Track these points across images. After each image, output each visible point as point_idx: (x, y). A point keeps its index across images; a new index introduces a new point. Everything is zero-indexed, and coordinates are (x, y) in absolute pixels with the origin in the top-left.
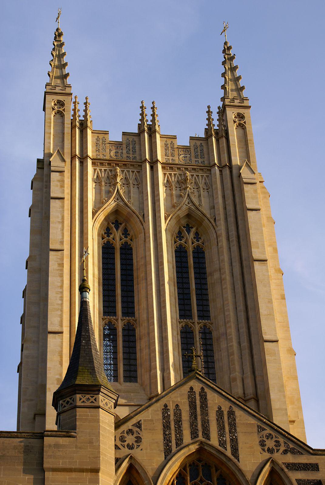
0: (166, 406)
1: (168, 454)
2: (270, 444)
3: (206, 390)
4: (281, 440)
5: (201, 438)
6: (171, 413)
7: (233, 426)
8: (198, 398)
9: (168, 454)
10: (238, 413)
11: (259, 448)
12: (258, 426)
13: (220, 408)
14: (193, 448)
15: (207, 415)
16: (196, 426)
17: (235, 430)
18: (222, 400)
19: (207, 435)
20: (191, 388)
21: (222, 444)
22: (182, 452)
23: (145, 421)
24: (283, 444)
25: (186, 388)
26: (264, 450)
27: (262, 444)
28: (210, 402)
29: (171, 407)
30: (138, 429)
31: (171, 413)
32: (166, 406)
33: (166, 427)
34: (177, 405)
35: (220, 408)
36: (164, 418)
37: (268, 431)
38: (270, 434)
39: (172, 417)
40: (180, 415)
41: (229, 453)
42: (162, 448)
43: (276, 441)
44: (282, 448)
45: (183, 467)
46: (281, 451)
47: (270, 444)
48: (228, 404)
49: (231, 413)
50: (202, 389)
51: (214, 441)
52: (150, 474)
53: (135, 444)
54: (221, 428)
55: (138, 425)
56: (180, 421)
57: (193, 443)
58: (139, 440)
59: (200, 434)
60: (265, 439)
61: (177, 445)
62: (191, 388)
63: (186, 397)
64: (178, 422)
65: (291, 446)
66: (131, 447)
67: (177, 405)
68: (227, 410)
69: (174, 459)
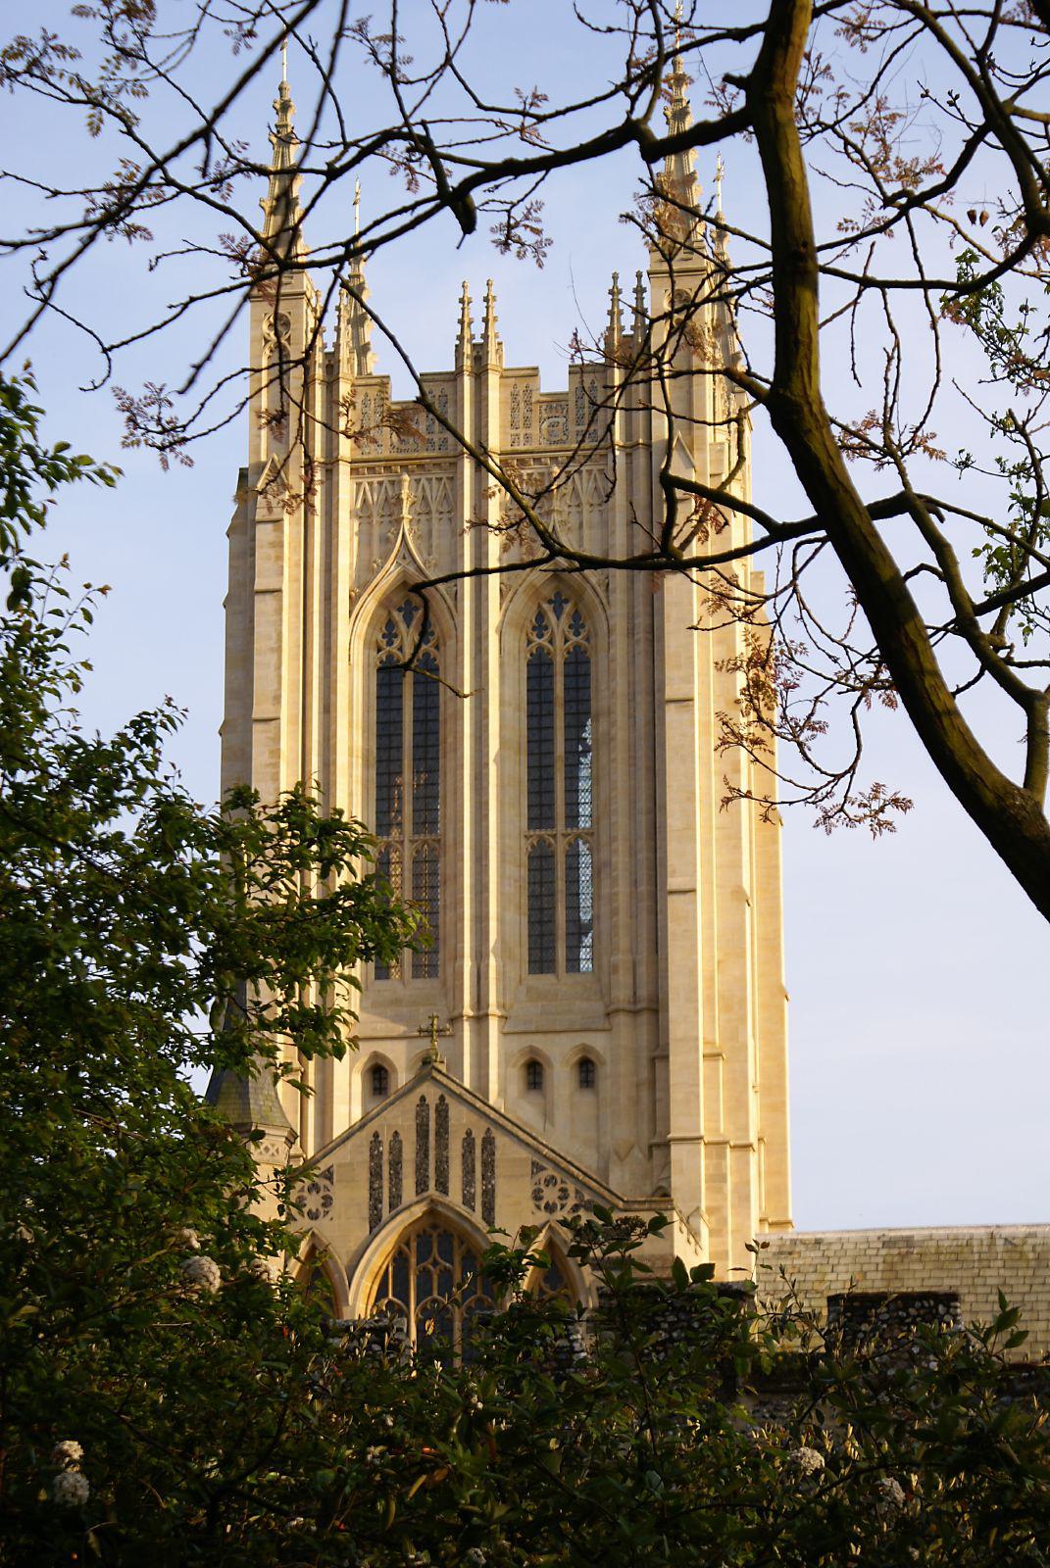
0: (376, 1135)
1: (376, 1223)
2: (551, 1195)
3: (448, 1100)
4: (571, 1187)
5: (432, 1190)
6: (385, 1148)
7: (489, 1166)
8: (433, 1115)
9: (376, 1223)
10: (501, 1140)
11: (531, 1204)
12: (533, 1163)
13: (469, 1133)
14: (418, 1211)
15: (446, 1147)
16: (426, 1170)
17: (493, 1172)
18: (475, 1117)
19: (443, 1186)
20: (423, 1099)
21: (468, 1200)
22: (399, 1218)
23: (339, 1166)
24: (572, 1194)
25: (413, 1099)
26: (538, 1207)
27: (537, 1196)
28: (452, 1122)
29: (386, 1138)
30: (327, 1183)
31: (385, 1148)
32: (376, 1135)
33: (375, 1174)
34: (396, 1133)
35: (469, 1133)
36: (372, 1156)
37: (550, 1171)
38: (553, 1177)
39: (386, 1157)
40: (400, 1150)
41: (477, 1217)
42: (366, 1213)
43: (562, 1190)
44: (571, 1202)
45: (404, 1241)
46: (568, 1207)
47: (551, 1195)
48: (484, 1125)
49: (488, 1142)
50: (442, 1098)
51: (455, 1196)
52: (342, 1261)
53: (322, 1210)
54: (468, 1172)
55: (328, 1175)
56: (400, 1162)
57: (417, 1202)
58: (327, 1201)
59: (432, 1184)
60: (542, 1187)
61: (392, 1206)
62: (423, 1099)
63: (413, 1114)
64: (396, 1164)
65: (587, 1197)
66: (313, 1216)
67: (396, 1133)
68: (482, 1135)
69: (383, 1233)
